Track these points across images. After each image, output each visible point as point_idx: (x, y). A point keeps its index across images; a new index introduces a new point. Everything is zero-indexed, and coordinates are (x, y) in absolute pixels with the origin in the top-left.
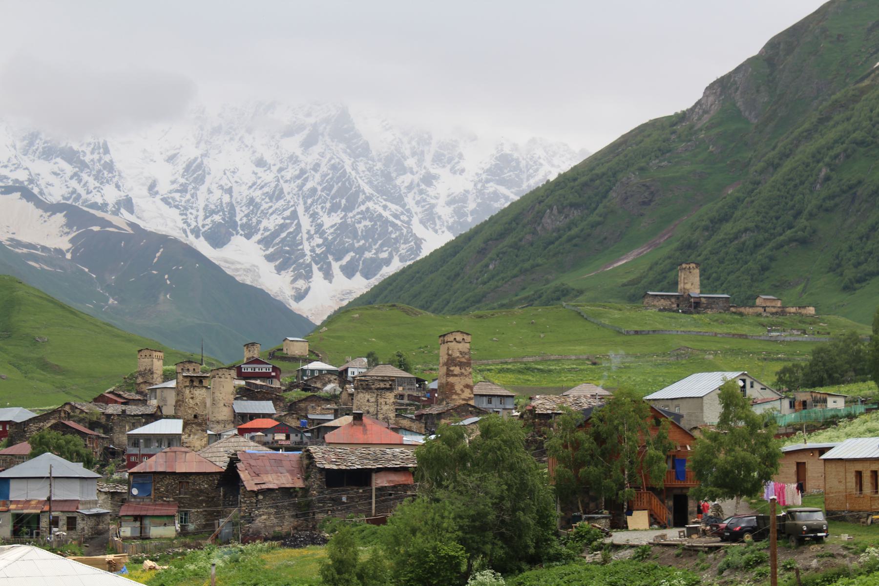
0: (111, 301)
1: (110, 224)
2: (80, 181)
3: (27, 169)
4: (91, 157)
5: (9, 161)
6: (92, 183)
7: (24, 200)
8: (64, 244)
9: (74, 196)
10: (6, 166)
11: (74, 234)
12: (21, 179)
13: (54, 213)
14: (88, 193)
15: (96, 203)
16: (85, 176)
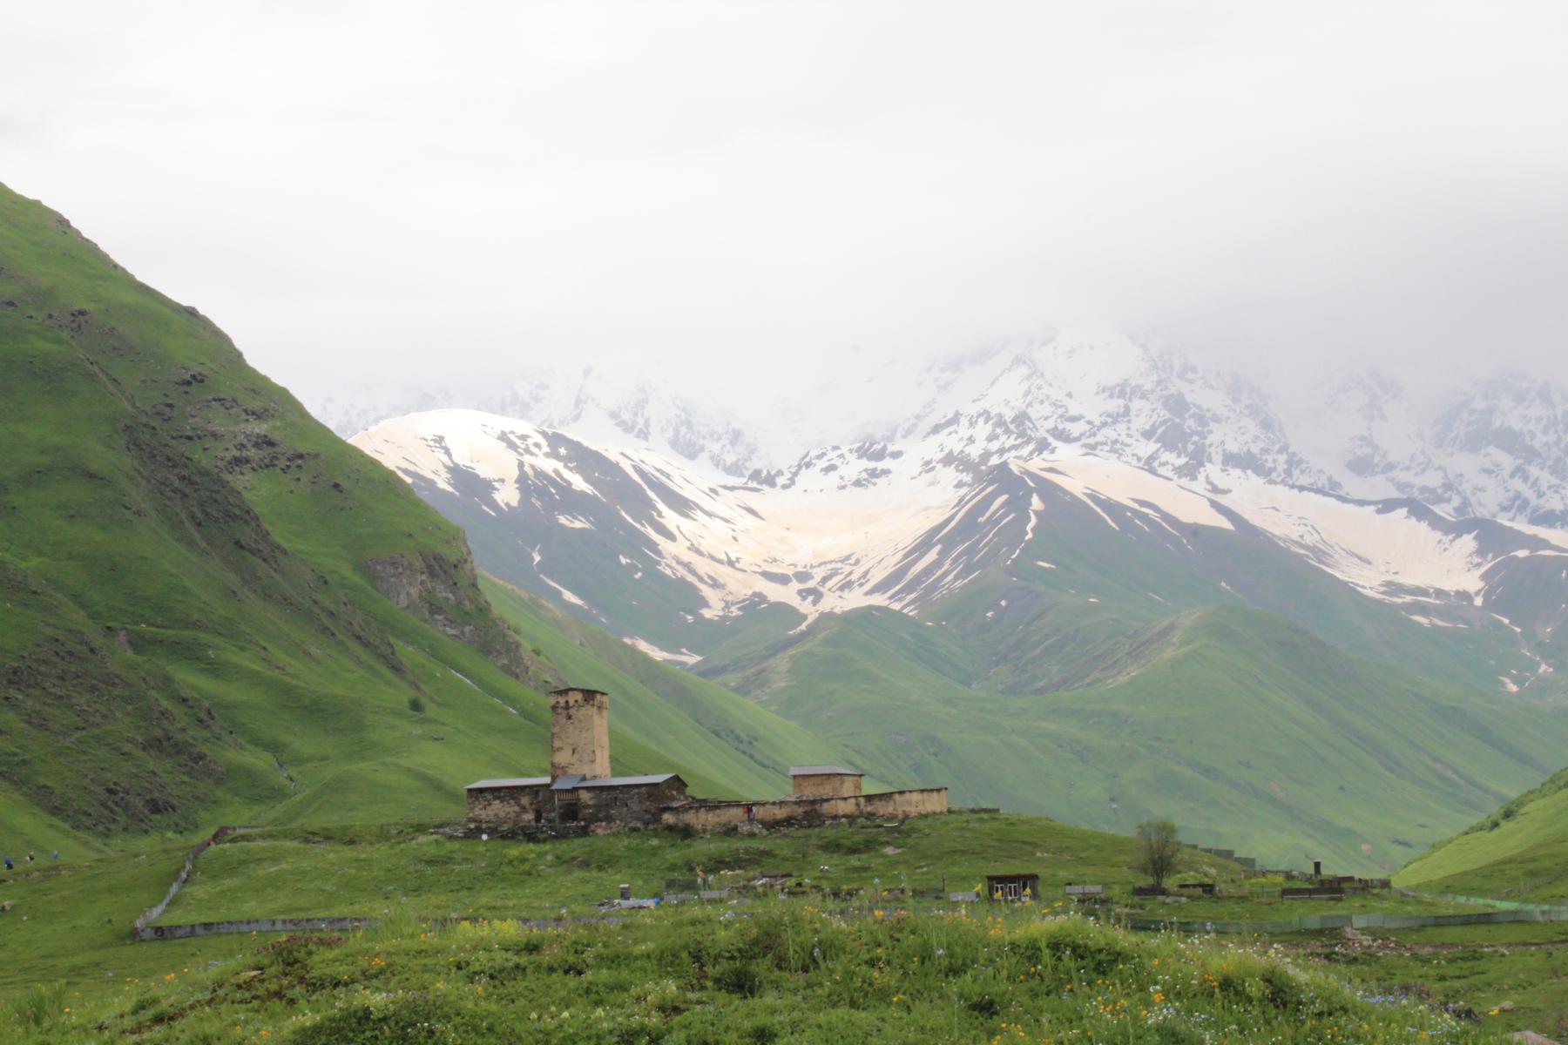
0: (1543, 668)
1: (1546, 544)
2: (1526, 479)
3: (1440, 468)
4: (1545, 439)
5: (1412, 460)
6: (1546, 478)
7: (1413, 520)
8: (1471, 582)
9: (1518, 503)
10: (1407, 468)
11: (1488, 566)
12: (1431, 486)
13: (1459, 535)
14: (1540, 495)
15: (1552, 512)
16: (1534, 471)
